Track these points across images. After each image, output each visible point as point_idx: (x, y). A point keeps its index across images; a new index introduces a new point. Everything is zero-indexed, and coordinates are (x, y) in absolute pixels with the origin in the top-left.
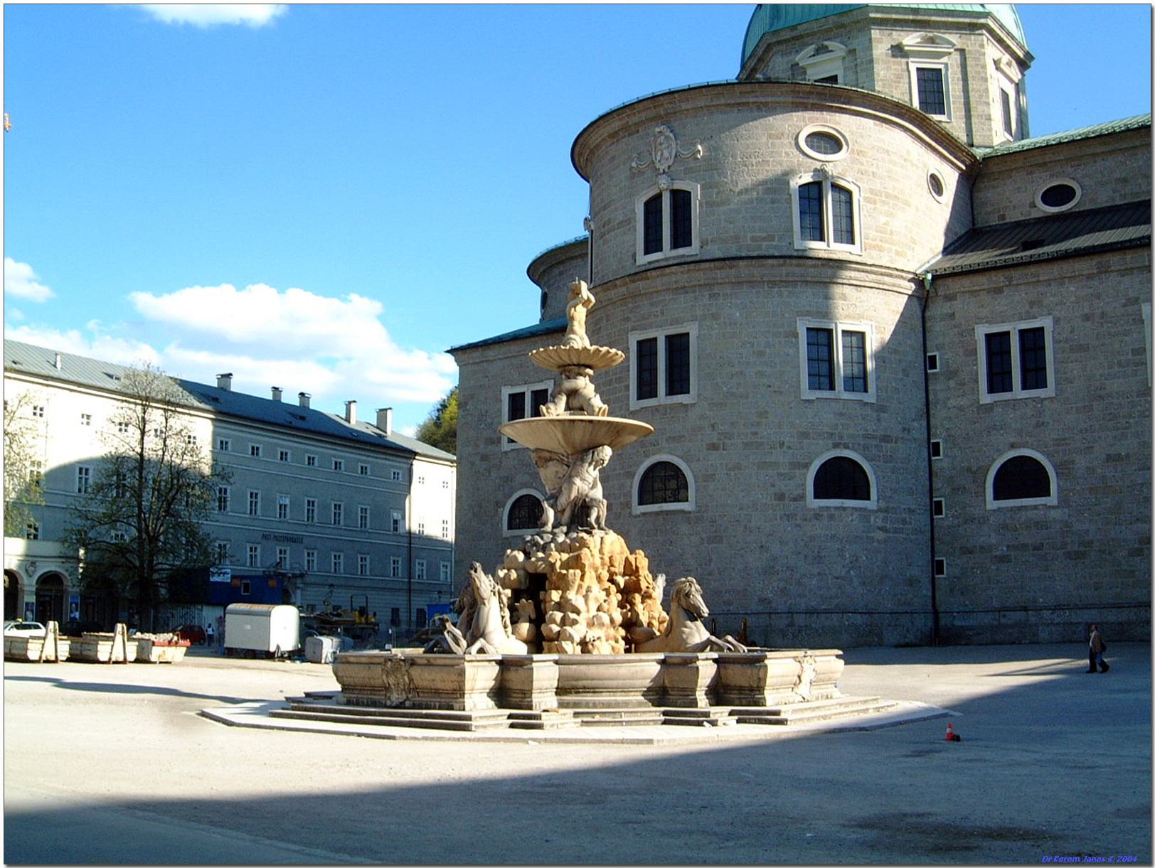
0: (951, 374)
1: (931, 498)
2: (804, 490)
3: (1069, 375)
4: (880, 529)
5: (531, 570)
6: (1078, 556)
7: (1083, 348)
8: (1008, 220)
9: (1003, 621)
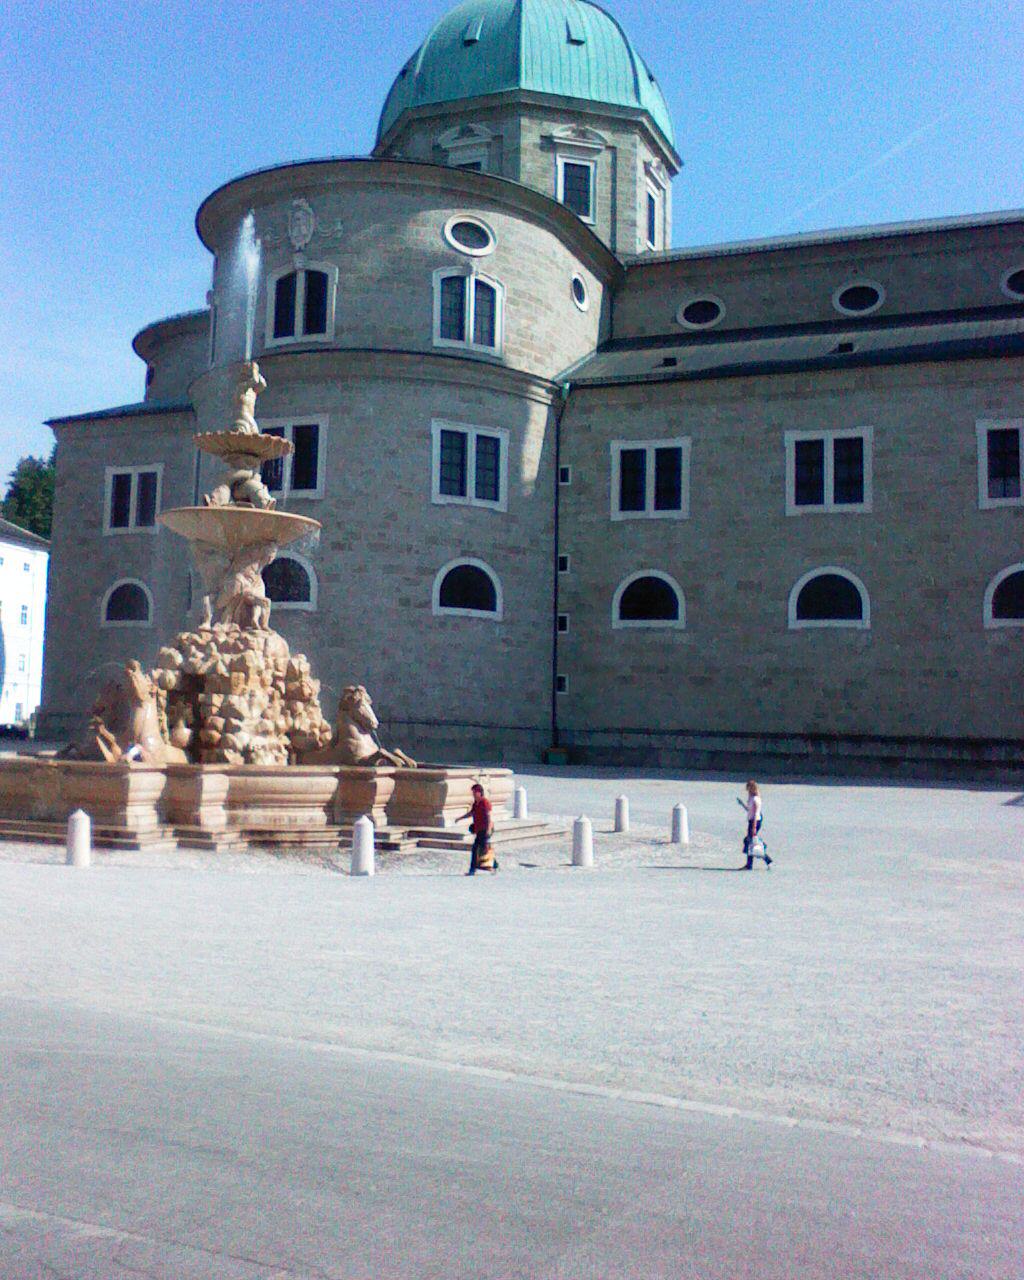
0: (582, 488)
1: (556, 613)
2: (430, 596)
4: (504, 641)
5: (189, 671)
6: (701, 682)
8: (647, 334)
9: (626, 743)
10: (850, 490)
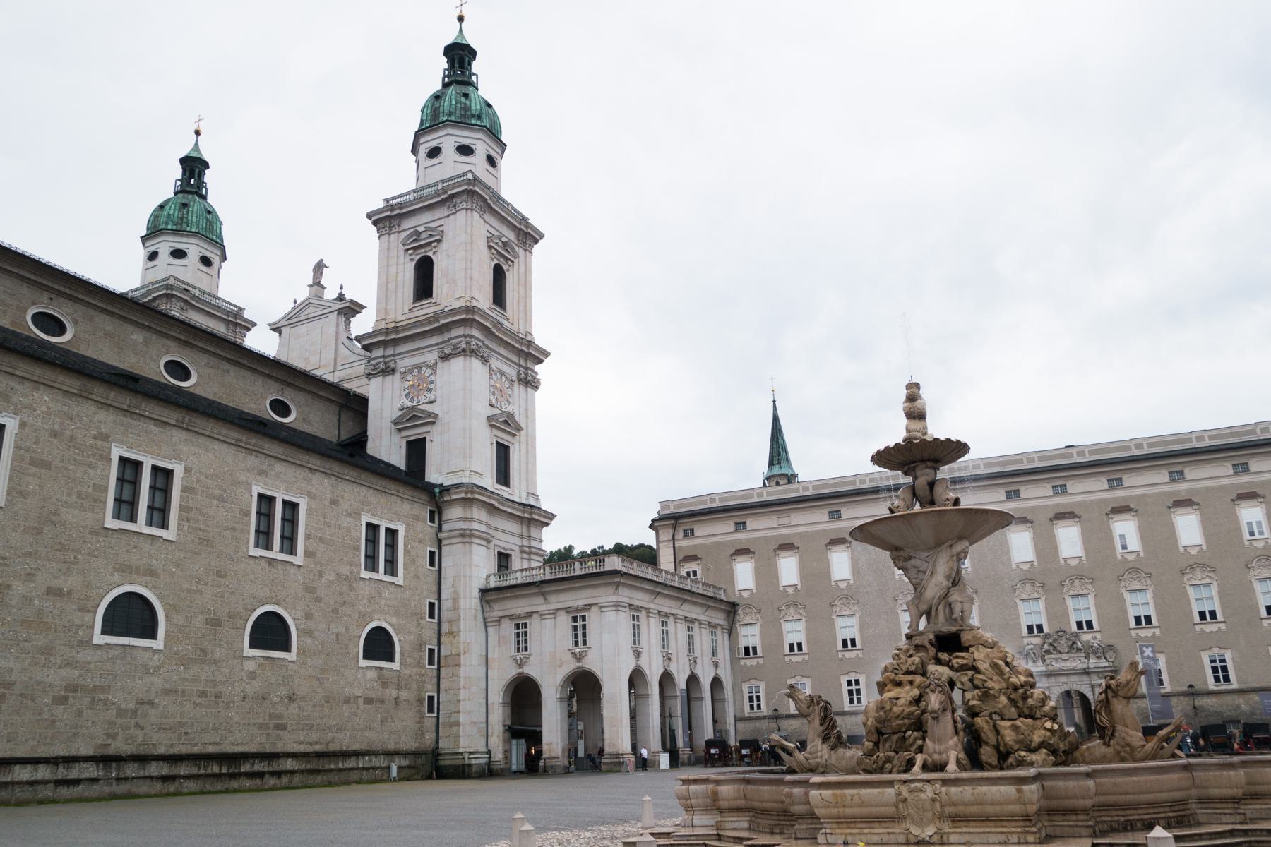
3: (23, 488)
7: (45, 465)
10: (159, 514)
